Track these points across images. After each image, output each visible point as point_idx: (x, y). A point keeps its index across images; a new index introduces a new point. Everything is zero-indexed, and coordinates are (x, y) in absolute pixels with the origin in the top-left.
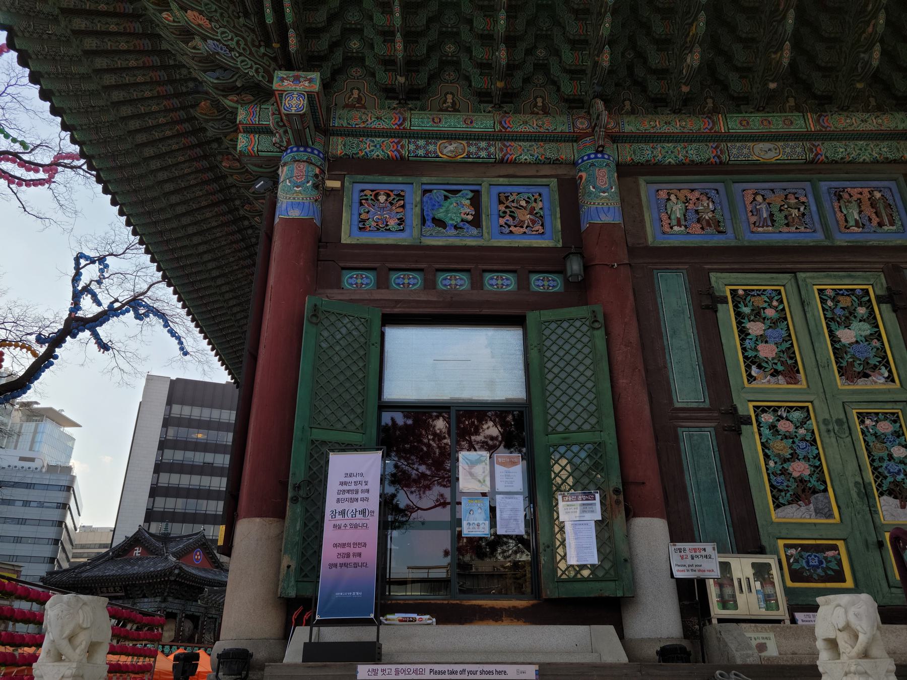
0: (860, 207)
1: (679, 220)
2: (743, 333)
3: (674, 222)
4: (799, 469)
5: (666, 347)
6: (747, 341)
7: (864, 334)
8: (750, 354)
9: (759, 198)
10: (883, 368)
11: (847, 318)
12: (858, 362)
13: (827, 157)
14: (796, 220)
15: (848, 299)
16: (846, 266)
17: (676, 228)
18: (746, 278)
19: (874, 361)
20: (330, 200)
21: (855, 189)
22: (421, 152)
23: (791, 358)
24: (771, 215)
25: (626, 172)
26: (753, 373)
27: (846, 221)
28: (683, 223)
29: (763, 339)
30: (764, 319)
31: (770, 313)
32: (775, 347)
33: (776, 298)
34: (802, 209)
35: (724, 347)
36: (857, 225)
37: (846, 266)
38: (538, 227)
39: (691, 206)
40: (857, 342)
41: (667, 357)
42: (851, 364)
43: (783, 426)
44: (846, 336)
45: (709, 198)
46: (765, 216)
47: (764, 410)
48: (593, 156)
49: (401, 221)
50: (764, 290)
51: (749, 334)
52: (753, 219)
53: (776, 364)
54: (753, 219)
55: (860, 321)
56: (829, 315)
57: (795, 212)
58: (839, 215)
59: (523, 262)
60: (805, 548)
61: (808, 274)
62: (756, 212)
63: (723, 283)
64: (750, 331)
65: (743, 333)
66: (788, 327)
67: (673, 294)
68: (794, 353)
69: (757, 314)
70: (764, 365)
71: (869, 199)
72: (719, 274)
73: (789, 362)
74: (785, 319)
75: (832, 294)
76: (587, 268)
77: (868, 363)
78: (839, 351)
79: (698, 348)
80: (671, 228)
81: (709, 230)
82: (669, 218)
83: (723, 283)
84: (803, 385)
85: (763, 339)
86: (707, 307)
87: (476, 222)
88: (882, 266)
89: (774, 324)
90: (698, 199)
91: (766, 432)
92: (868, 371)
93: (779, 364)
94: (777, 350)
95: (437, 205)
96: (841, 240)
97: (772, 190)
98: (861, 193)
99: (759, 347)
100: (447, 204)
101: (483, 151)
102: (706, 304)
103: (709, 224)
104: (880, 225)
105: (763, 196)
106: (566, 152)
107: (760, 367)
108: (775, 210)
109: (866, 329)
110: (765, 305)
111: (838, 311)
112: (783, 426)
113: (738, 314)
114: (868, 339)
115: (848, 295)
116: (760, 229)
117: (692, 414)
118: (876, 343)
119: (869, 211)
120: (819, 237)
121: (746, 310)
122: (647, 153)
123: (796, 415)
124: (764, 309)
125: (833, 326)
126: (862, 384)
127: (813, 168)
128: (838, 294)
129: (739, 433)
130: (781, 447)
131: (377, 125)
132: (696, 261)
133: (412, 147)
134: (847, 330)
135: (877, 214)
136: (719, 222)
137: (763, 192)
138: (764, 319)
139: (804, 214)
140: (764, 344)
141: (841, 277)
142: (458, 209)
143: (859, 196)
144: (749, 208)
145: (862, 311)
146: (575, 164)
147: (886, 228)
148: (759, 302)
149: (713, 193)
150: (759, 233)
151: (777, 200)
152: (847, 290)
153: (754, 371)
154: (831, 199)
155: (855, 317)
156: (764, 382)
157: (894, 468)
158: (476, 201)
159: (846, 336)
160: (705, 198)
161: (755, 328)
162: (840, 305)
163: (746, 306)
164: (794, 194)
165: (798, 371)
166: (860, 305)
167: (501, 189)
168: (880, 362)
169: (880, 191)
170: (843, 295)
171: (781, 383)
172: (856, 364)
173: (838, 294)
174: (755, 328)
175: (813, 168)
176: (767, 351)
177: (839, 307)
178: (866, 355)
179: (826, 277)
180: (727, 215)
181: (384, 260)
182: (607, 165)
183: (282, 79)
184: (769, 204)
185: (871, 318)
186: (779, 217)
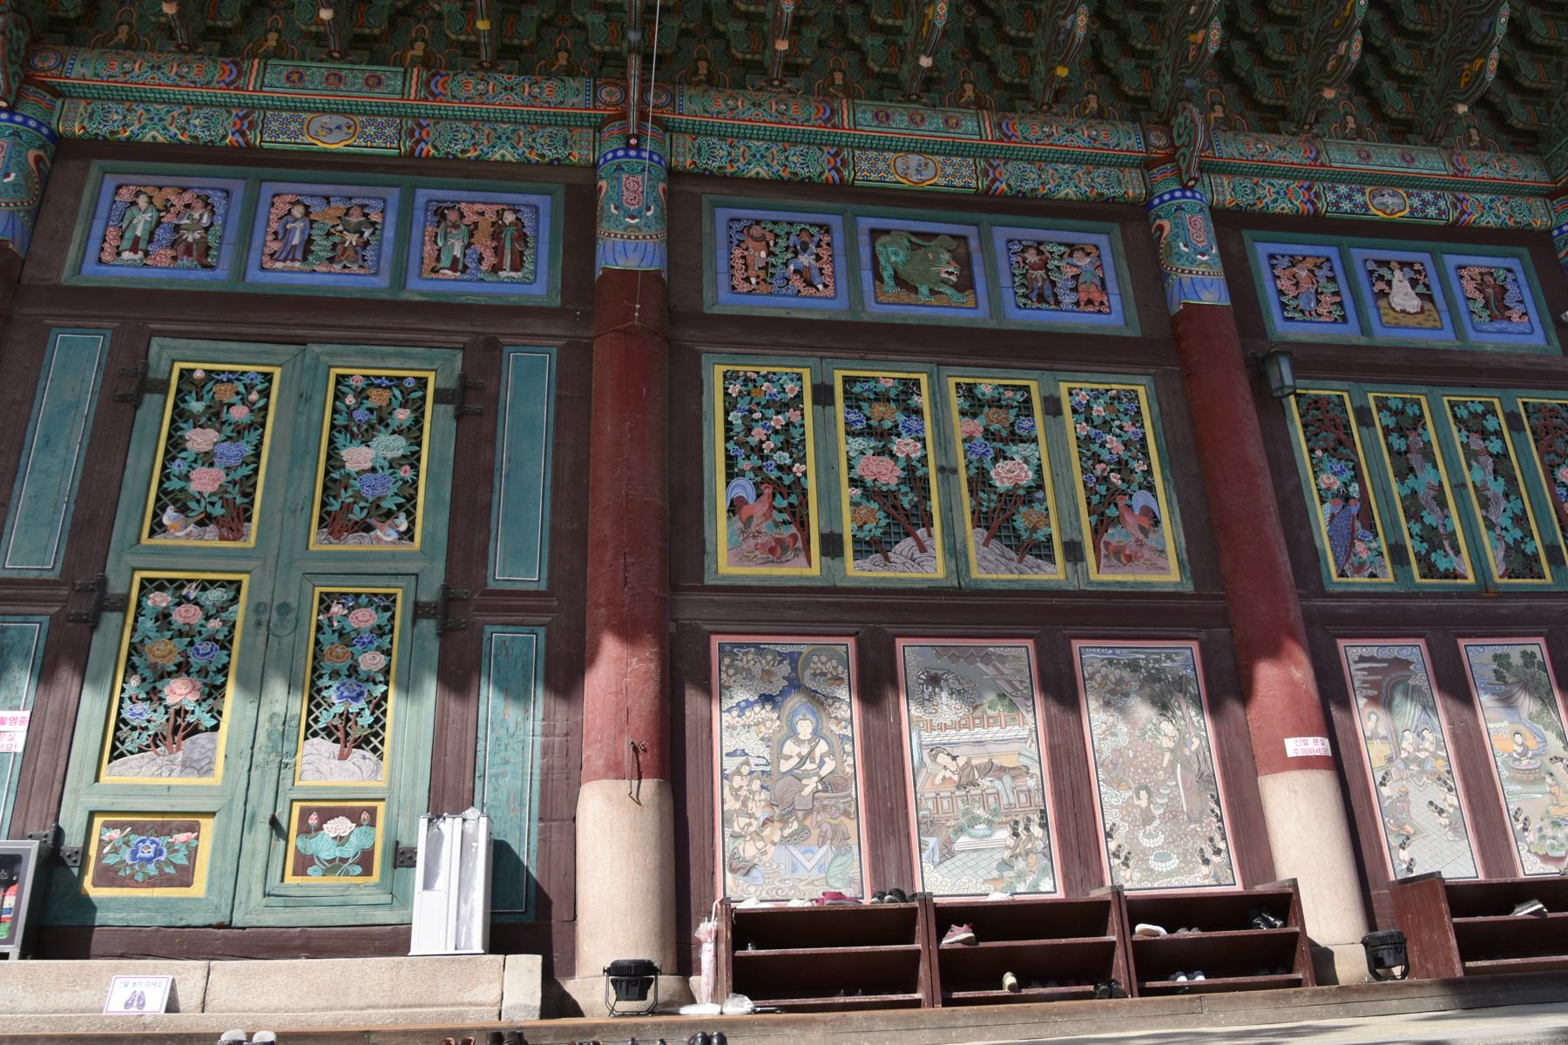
0: (471, 235)
1: (136, 240)
2: (176, 445)
3: (126, 244)
5: (21, 469)
6: (178, 461)
7: (389, 455)
9: (298, 212)
10: (402, 516)
11: (372, 427)
12: (362, 504)
13: (1009, 186)
14: (350, 252)
15: (387, 394)
16: (402, 336)
17: (127, 255)
18: (216, 350)
21: (478, 207)
23: (245, 495)
24: (309, 241)
26: (165, 520)
27: (438, 259)
28: (142, 245)
29: (208, 459)
30: (223, 423)
32: (223, 473)
33: (260, 387)
34: (367, 234)
35: (128, 473)
36: (453, 268)
37: (402, 336)
39: (169, 218)
40: (373, 470)
41: (17, 487)
42: (347, 508)
43: (183, 616)
45: (207, 204)
46: (296, 241)
47: (161, 586)
48: (621, 153)
50: (243, 373)
51: (185, 450)
52: (275, 246)
53: (213, 504)
54: (275, 246)
55: (394, 432)
56: (341, 420)
57: (352, 239)
58: (428, 248)
61: (327, 348)
62: (282, 235)
64: (188, 445)
65: (176, 445)
66: (261, 442)
68: (254, 486)
69: (214, 416)
70: (192, 505)
71: (493, 224)
72: (168, 341)
73: (239, 500)
74: (263, 425)
75: (361, 385)
77: (378, 506)
79: (79, 472)
80: (119, 254)
81: (185, 261)
82: (122, 237)
84: (251, 540)
85: (208, 459)
86: (123, 399)
88: (466, 339)
89: (240, 431)
90: (187, 206)
91: (148, 624)
92: (372, 521)
93: (219, 504)
94: (224, 479)
96: (418, 287)
97: (327, 198)
98: (482, 214)
99: (193, 475)
103: (189, 250)
104: (496, 269)
105: (306, 207)
107: (183, 509)
108: (317, 235)
109: (396, 446)
110: (236, 399)
111: (360, 415)
114: (393, 464)
115: (390, 388)
116: (279, 265)
118: (406, 473)
119: (484, 245)
120: (378, 283)
124: (230, 405)
125: (341, 439)
126: (353, 544)
127: (409, 168)
128: (372, 384)
129: (93, 624)
132: (135, 312)
134: (363, 448)
135: (498, 252)
136: (209, 248)
137: (308, 201)
138: (223, 423)
139: (367, 243)
140: (205, 469)
141: (384, 356)
143: (475, 218)
144: (275, 226)
145: (403, 416)
147: (503, 274)
148: (224, 393)
149: (217, 199)
150: (275, 270)
151: (326, 216)
152: (389, 378)
153: (169, 516)
154: (426, 220)
155: (387, 426)
159: (356, 457)
160: (200, 204)
161: (199, 439)
162: (368, 404)
163: (200, 399)
164: (363, 206)
165: (249, 520)
166: (403, 406)
168: (400, 506)
169: (516, 212)
170: (379, 386)
171: (211, 539)
172: (356, 508)
173: (372, 384)
174: (199, 439)
175: (409, 168)
176: (205, 481)
177: (364, 407)
178: (379, 492)
179: (357, 353)
180: (231, 236)
182: (16, 134)
184: (312, 222)
185: (413, 432)
186: (321, 246)
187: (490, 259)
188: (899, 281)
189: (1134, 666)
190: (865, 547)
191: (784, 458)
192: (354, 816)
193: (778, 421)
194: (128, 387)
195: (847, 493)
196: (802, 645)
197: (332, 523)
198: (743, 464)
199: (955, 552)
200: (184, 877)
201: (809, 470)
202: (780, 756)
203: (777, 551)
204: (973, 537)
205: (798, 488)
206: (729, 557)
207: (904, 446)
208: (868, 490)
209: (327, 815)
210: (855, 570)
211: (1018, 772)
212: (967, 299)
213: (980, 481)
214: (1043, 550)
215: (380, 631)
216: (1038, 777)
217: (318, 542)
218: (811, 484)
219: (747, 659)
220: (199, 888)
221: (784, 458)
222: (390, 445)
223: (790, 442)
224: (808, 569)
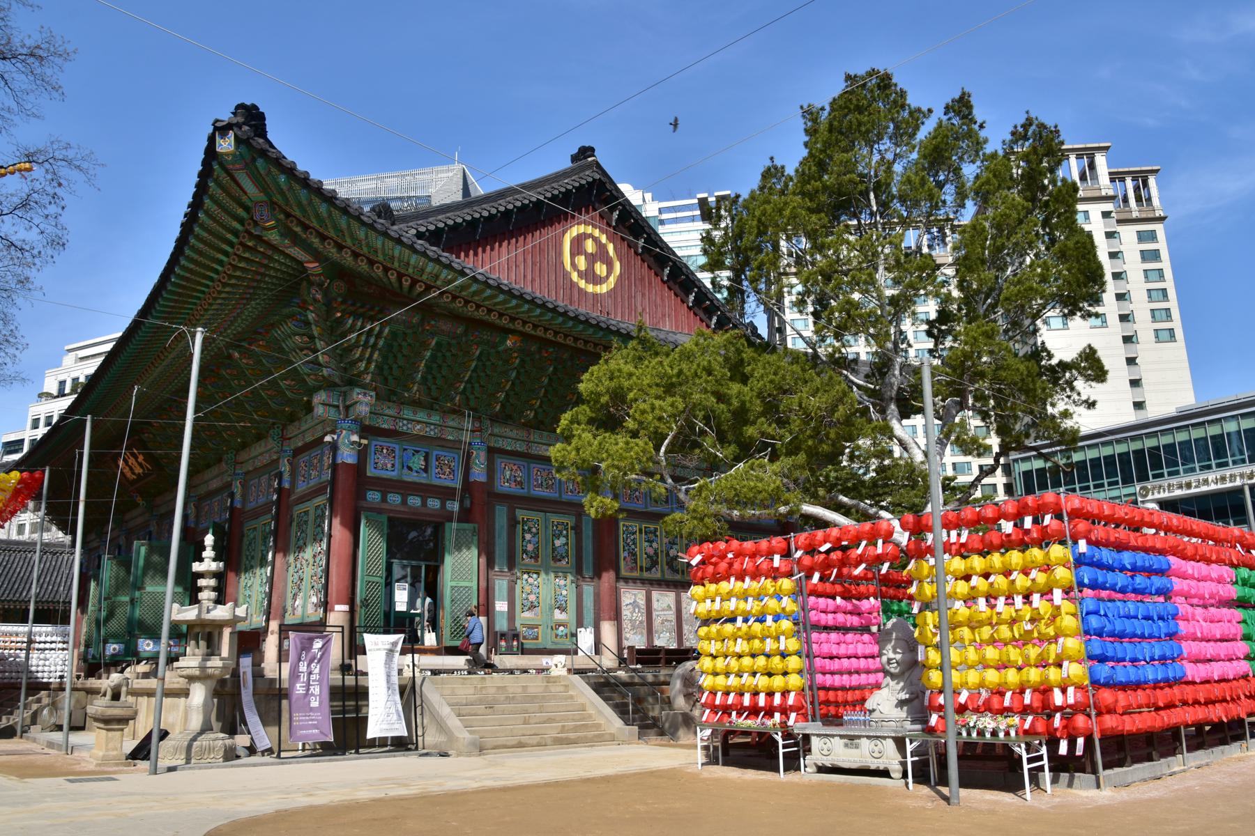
2: (523, 537)
4: (532, 598)
20: (362, 454)
25: (492, 452)
29: (530, 542)
31: (534, 530)
44: (558, 543)
49: (393, 465)
59: (446, 493)
63: (521, 514)
67: (501, 516)
69: (529, 531)
76: (472, 503)
78: (554, 549)
83: (521, 514)
102: (513, 523)
122: (501, 444)
130: (528, 589)
142: (418, 462)
156: (527, 560)
158: (426, 459)
159: (558, 543)
161: (528, 536)
174: (528, 536)
176: (530, 547)
181: (386, 486)
190: (648, 569)
199: (662, 571)
203: (632, 569)
204: (666, 567)
205: (635, 555)
207: (655, 545)
208: (649, 556)
210: (646, 575)
213: (668, 554)
214: (677, 571)
216: (674, 623)
222: (563, 540)
223: (635, 544)
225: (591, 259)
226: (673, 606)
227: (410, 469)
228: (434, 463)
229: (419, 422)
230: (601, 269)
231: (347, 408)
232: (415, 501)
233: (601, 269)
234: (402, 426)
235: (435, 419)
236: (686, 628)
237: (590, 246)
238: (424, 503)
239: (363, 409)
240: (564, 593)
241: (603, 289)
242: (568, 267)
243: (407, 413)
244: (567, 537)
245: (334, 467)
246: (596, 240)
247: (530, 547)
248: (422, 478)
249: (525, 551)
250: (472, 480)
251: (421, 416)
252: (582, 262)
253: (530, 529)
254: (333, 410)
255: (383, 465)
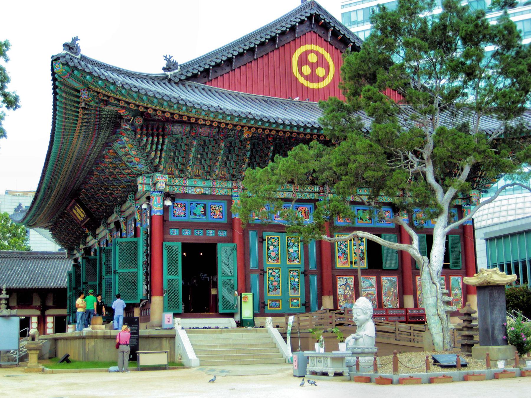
4: (275, 284)
8: (269, 255)
19: (296, 257)
22: (190, 192)
29: (273, 251)
31: (275, 244)
38: (221, 216)
43: (273, 274)
44: (291, 250)
47: (270, 269)
49: (185, 214)
59: (217, 227)
60: (273, 301)
67: (253, 236)
83: (266, 236)
84: (280, 263)
87: (205, 214)
91: (269, 275)
95: (194, 208)
100: (197, 208)
101: (208, 192)
102: (262, 240)
106: (229, 192)
112: (273, 274)
113: (268, 244)
117: (254, 271)
118: (297, 252)
121: (270, 243)
123: (277, 271)
126: (292, 263)
130: (272, 278)
131: (178, 184)
133: (187, 190)
135: (305, 215)
142: (200, 210)
146: (232, 196)
153: (269, 259)
156: (271, 262)
157: (295, 283)
158: (205, 207)
159: (291, 250)
167: (212, 203)
174: (271, 248)
176: (273, 254)
183: (158, 177)
187: (305, 217)
188: (361, 219)
189: (389, 280)
191: (345, 249)
192: (297, 299)
193: (344, 243)
194: (262, 240)
195: (354, 255)
196: (348, 277)
197: (289, 260)
198: (340, 251)
200: (279, 307)
201: (348, 251)
202: (345, 292)
203: (344, 264)
206: (339, 264)
209: (294, 299)
211: (373, 294)
212: (370, 222)
215: (297, 276)
217: (288, 263)
218: (349, 253)
219: (341, 279)
220: (281, 308)
221: (345, 249)
222: (295, 248)
224: (348, 266)
225: (313, 67)
226: (375, 285)
227: (195, 214)
228: (208, 209)
229: (198, 187)
230: (320, 72)
231: (155, 184)
232: (199, 233)
233: (320, 72)
234: (188, 191)
235: (209, 183)
236: (384, 298)
237: (313, 58)
238: (205, 233)
239: (161, 186)
240: (296, 280)
241: (321, 85)
242: (298, 76)
243: (191, 183)
244: (298, 246)
245: (151, 217)
246: (317, 53)
247: (273, 254)
248: (203, 219)
249: (269, 257)
250: (233, 217)
251: (200, 183)
252: (307, 70)
253: (272, 244)
254: (147, 187)
255: (179, 213)
